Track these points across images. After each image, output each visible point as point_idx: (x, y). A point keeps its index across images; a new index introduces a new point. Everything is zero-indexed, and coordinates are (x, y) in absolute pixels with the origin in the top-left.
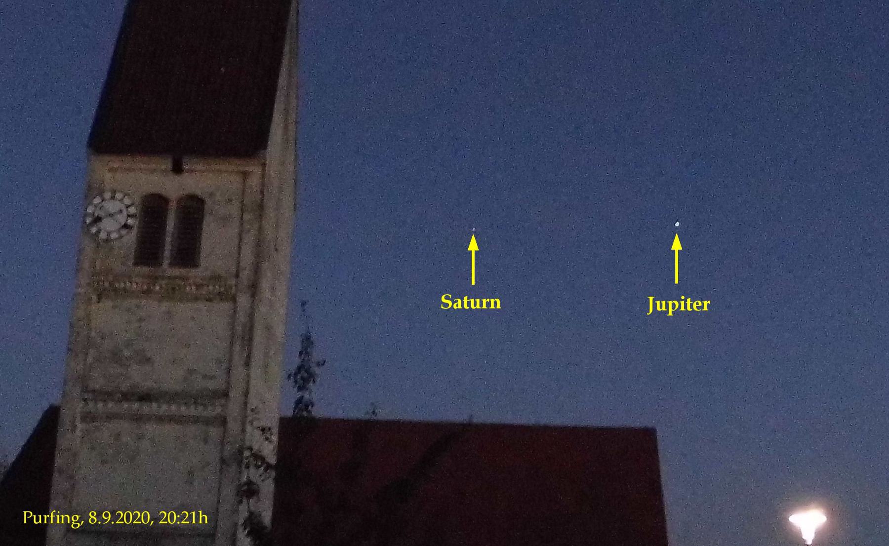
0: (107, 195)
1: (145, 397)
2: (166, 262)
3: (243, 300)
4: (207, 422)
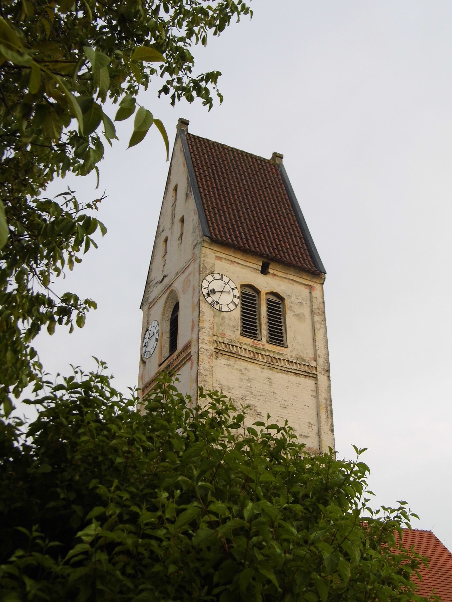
0: (217, 276)
3: (322, 378)
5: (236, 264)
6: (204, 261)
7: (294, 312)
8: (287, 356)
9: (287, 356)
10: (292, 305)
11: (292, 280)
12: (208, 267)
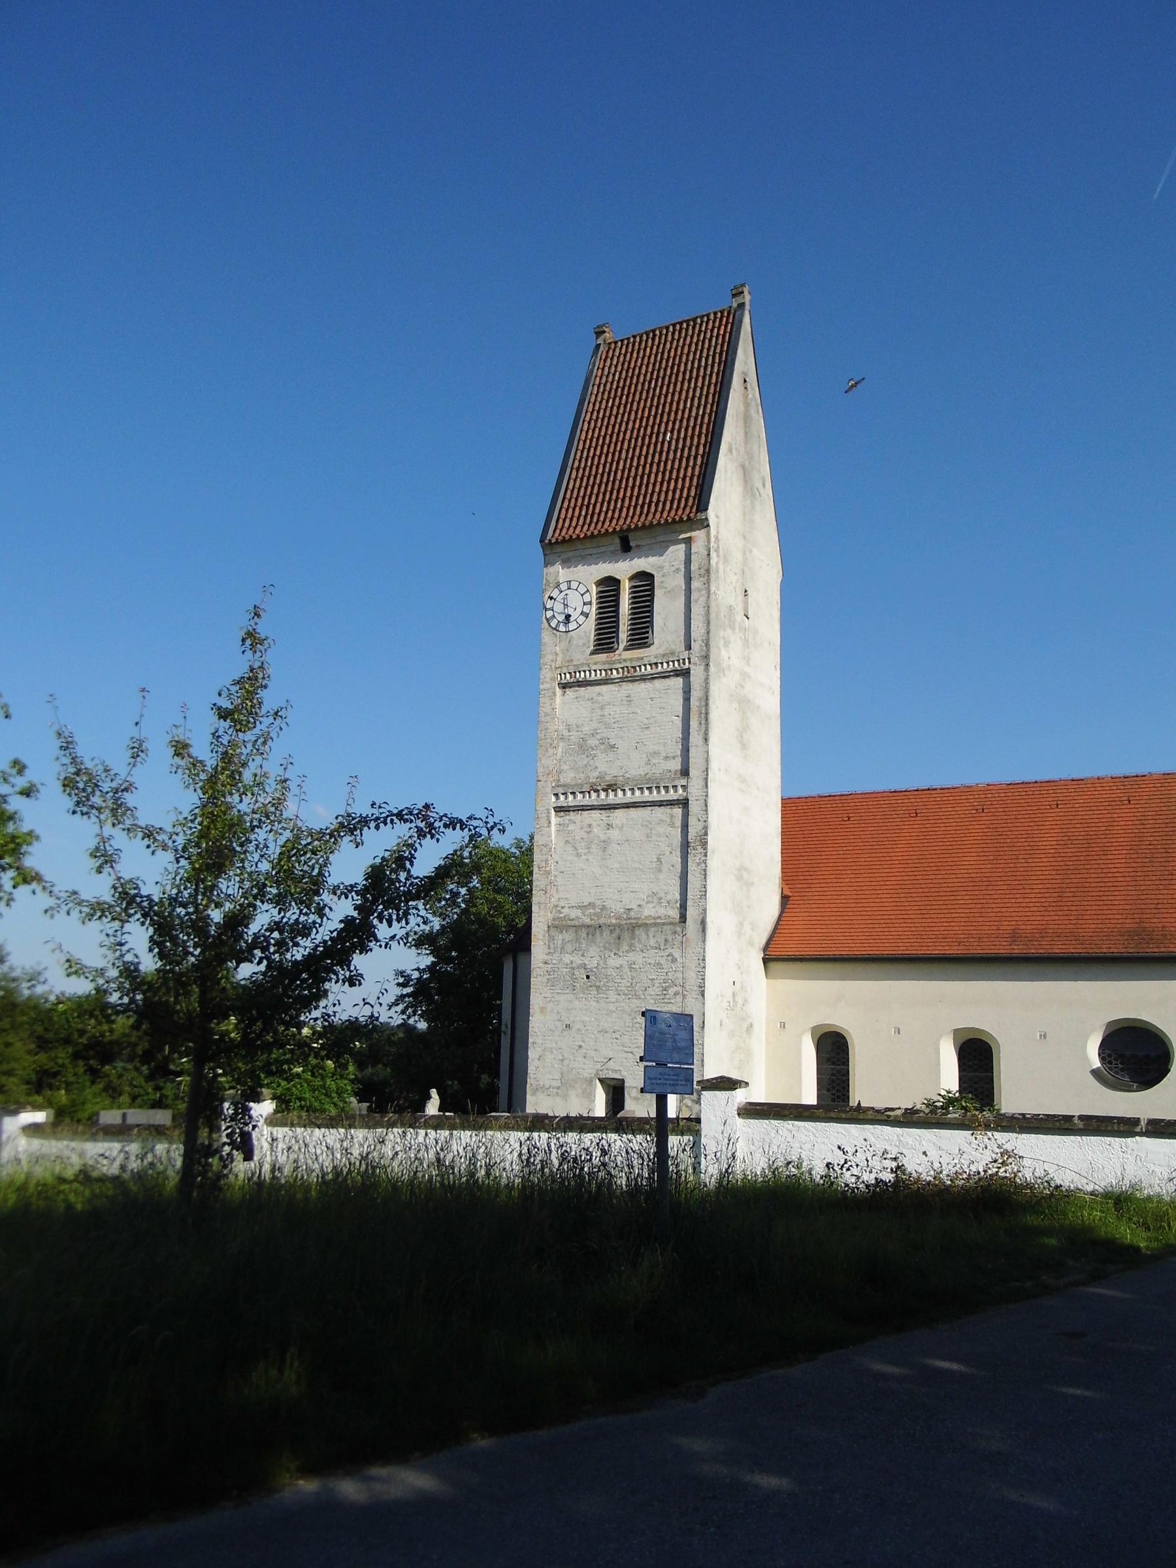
1: (611, 787)
2: (622, 646)
4: (671, 803)
7: (666, 588)
8: (648, 659)
9: (648, 659)
10: (663, 579)
12: (551, 579)
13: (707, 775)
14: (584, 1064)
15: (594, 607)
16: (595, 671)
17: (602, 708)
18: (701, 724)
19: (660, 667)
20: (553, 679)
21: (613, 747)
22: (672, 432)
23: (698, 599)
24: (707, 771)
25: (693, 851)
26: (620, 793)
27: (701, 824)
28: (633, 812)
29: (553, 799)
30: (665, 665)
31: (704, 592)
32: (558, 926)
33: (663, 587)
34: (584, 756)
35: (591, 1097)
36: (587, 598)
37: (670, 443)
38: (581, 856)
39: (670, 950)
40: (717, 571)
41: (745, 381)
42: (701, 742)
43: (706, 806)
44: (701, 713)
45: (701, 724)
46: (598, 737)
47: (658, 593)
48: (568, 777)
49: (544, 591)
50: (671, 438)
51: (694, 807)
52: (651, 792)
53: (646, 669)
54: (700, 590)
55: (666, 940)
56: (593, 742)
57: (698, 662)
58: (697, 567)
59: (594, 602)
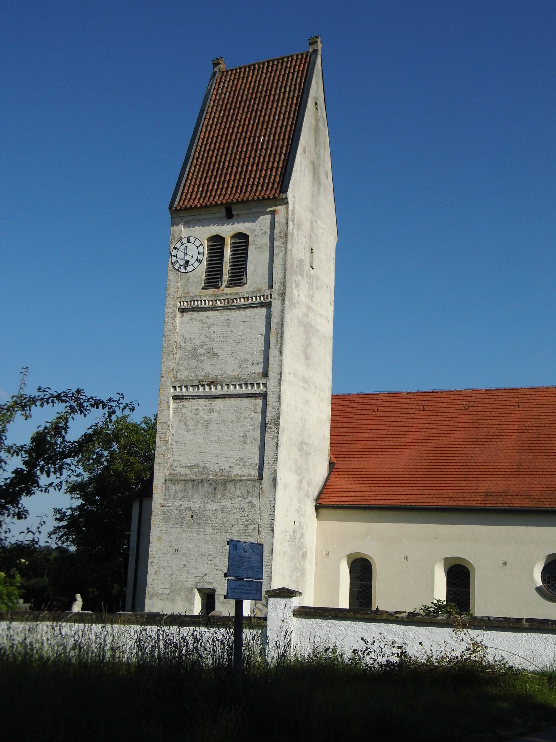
1: (213, 383)
2: (224, 285)
5: (203, 221)
6: (173, 231)
7: (257, 245)
9: (243, 293)
10: (255, 239)
11: (256, 212)
12: (176, 235)
13: (281, 376)
14: (187, 578)
15: (206, 256)
16: (205, 301)
17: (209, 327)
18: (277, 341)
19: (250, 301)
20: (175, 305)
21: (215, 355)
22: (264, 136)
23: (279, 254)
24: (281, 374)
25: (269, 430)
26: (219, 388)
27: (276, 411)
28: (228, 401)
29: (172, 390)
30: (254, 299)
31: (283, 249)
32: (172, 480)
33: (255, 244)
34: (195, 361)
35: (191, 601)
36: (201, 249)
37: (263, 144)
38: (190, 431)
39: (251, 499)
40: (293, 235)
41: (316, 104)
42: (277, 354)
43: (279, 398)
44: (278, 333)
45: (277, 341)
46: (205, 347)
47: (251, 248)
48: (183, 375)
49: (171, 243)
50: (264, 140)
51: (271, 399)
52: (241, 388)
53: (240, 301)
54: (280, 248)
55: (248, 492)
56: (201, 351)
57: (277, 298)
58: (278, 231)
59: (206, 252)
